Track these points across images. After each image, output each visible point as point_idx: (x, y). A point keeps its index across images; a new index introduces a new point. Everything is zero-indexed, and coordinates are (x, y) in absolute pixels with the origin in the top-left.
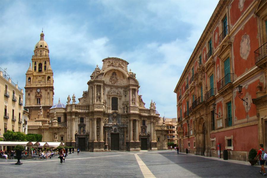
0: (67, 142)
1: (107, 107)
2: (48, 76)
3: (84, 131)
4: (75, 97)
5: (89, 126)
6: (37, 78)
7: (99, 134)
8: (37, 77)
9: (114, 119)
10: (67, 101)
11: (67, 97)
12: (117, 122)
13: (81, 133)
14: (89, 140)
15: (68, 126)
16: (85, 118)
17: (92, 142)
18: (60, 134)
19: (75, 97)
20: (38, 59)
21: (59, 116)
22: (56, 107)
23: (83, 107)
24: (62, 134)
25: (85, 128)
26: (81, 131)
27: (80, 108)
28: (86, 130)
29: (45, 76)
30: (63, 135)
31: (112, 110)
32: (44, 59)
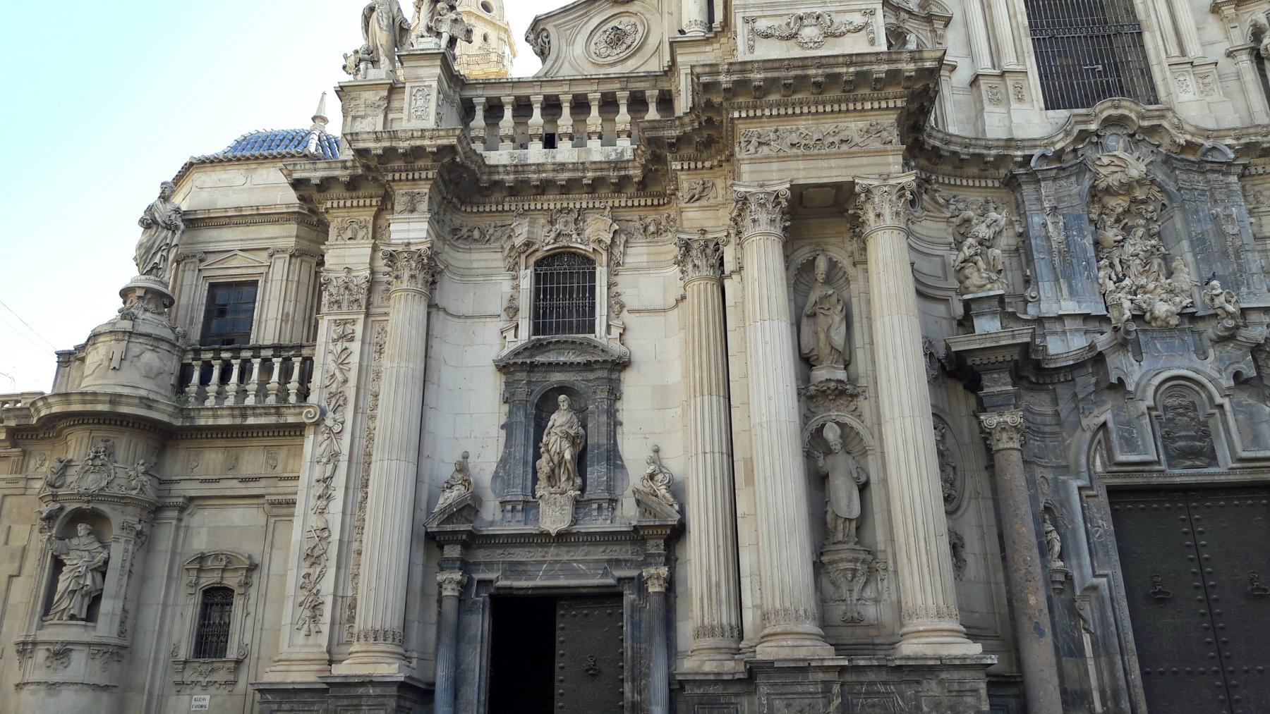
0: (272, 676)
1: (963, 75)
3: (596, 472)
5: (675, 374)
7: (864, 488)
9: (1111, 234)
12: (1186, 276)
13: (529, 506)
14: (686, 630)
15: (313, 398)
16: (615, 267)
17: (732, 667)
18: (200, 543)
21: (236, 269)
23: (581, 106)
24: (225, 546)
25: (612, 413)
26: (544, 465)
27: (537, 118)
28: (633, 450)
30: (228, 562)
31: (1051, 104)
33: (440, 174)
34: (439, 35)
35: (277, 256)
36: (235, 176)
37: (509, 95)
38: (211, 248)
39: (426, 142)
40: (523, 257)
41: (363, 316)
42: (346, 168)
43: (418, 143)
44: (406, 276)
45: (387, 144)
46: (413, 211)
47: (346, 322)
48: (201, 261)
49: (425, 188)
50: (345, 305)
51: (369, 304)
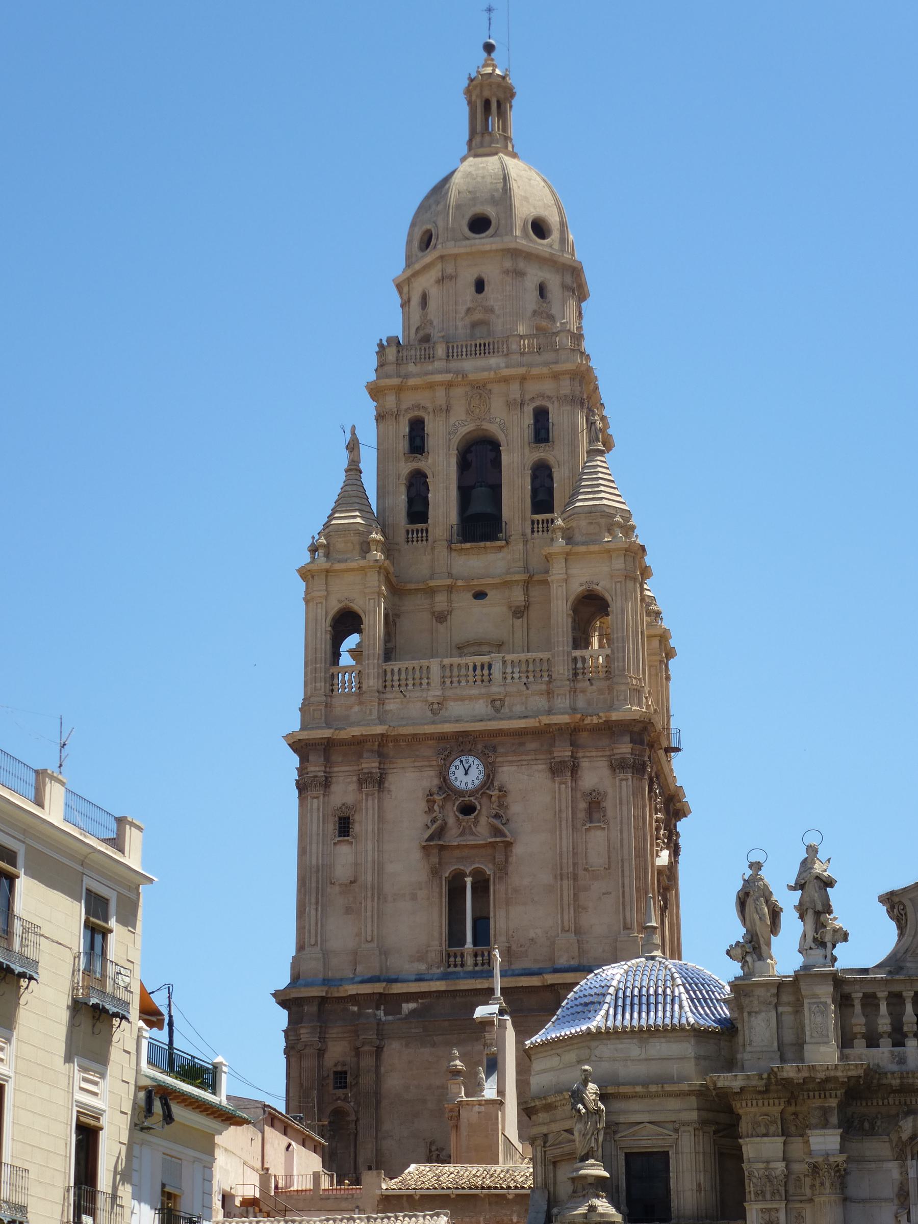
2: (577, 588)
4: (829, 883)
6: (441, 618)
8: (441, 602)
10: (738, 933)
11: (739, 885)
19: (829, 883)
20: (449, 385)
22: (597, 1022)
29: (535, 592)
32: (523, 379)
33: (846, 1093)
34: (823, 944)
35: (682, 1129)
36: (633, 1049)
37: (883, 991)
38: (622, 1120)
39: (839, 1074)
40: (909, 1149)
41: (783, 1205)
42: (762, 1079)
43: (832, 1074)
44: (827, 1184)
45: (805, 1074)
46: (825, 1125)
47: (769, 1210)
48: (615, 1132)
49: (835, 1105)
50: (768, 1196)
51: (786, 1191)
